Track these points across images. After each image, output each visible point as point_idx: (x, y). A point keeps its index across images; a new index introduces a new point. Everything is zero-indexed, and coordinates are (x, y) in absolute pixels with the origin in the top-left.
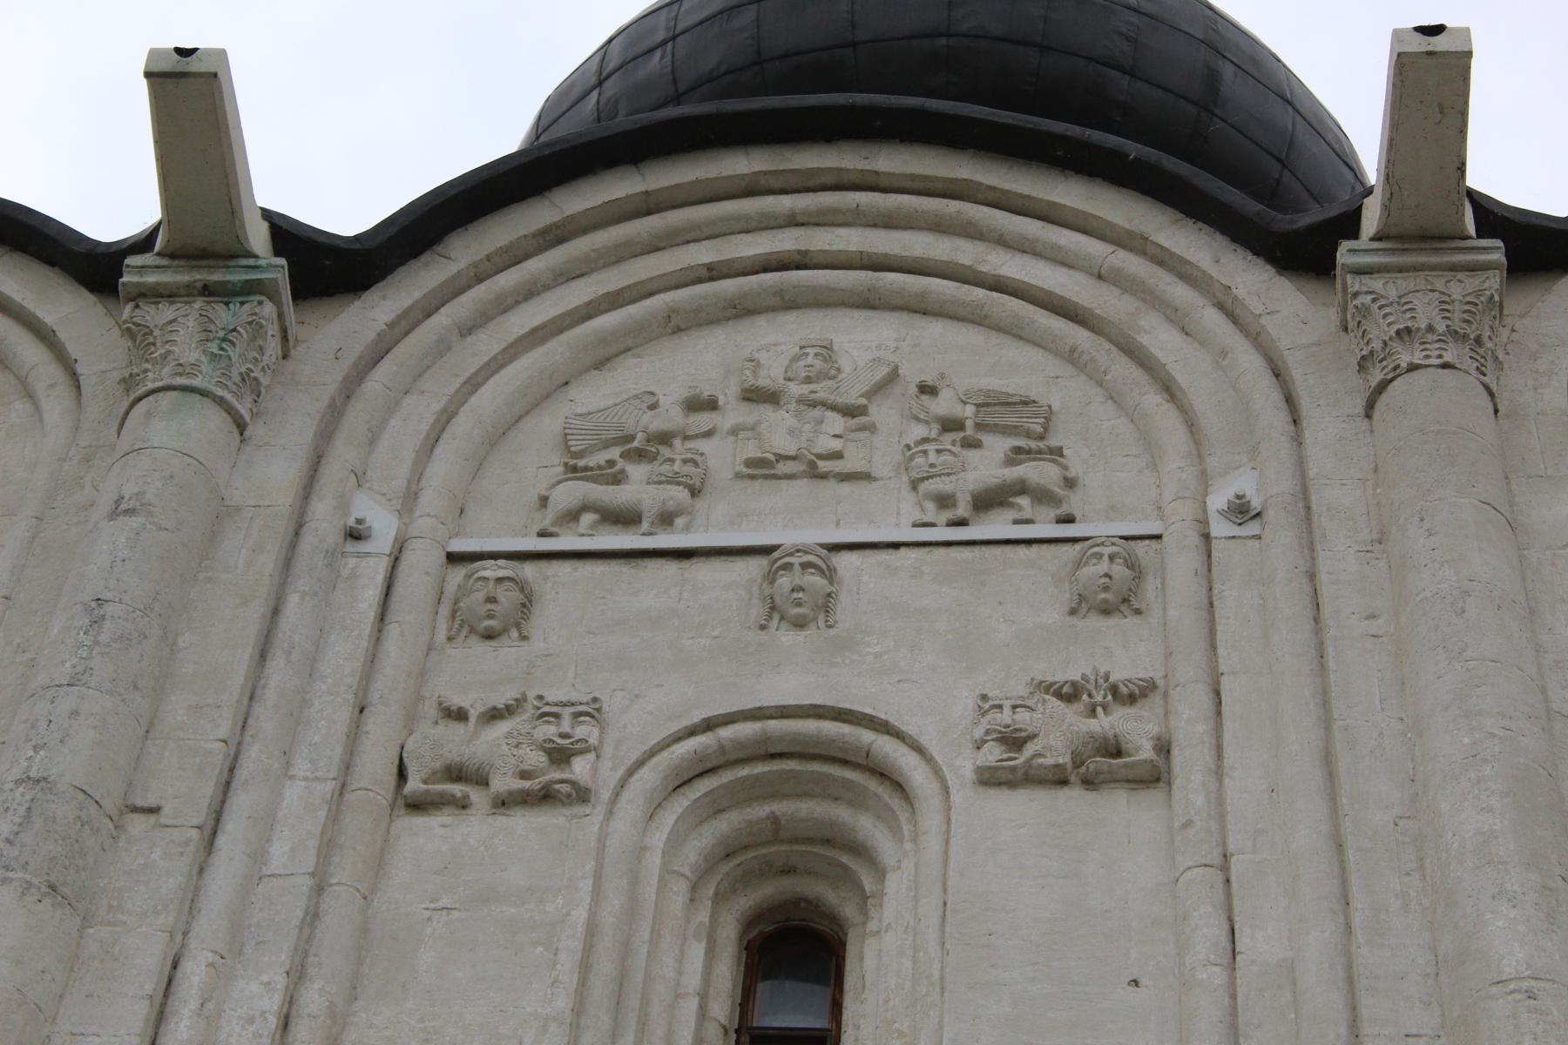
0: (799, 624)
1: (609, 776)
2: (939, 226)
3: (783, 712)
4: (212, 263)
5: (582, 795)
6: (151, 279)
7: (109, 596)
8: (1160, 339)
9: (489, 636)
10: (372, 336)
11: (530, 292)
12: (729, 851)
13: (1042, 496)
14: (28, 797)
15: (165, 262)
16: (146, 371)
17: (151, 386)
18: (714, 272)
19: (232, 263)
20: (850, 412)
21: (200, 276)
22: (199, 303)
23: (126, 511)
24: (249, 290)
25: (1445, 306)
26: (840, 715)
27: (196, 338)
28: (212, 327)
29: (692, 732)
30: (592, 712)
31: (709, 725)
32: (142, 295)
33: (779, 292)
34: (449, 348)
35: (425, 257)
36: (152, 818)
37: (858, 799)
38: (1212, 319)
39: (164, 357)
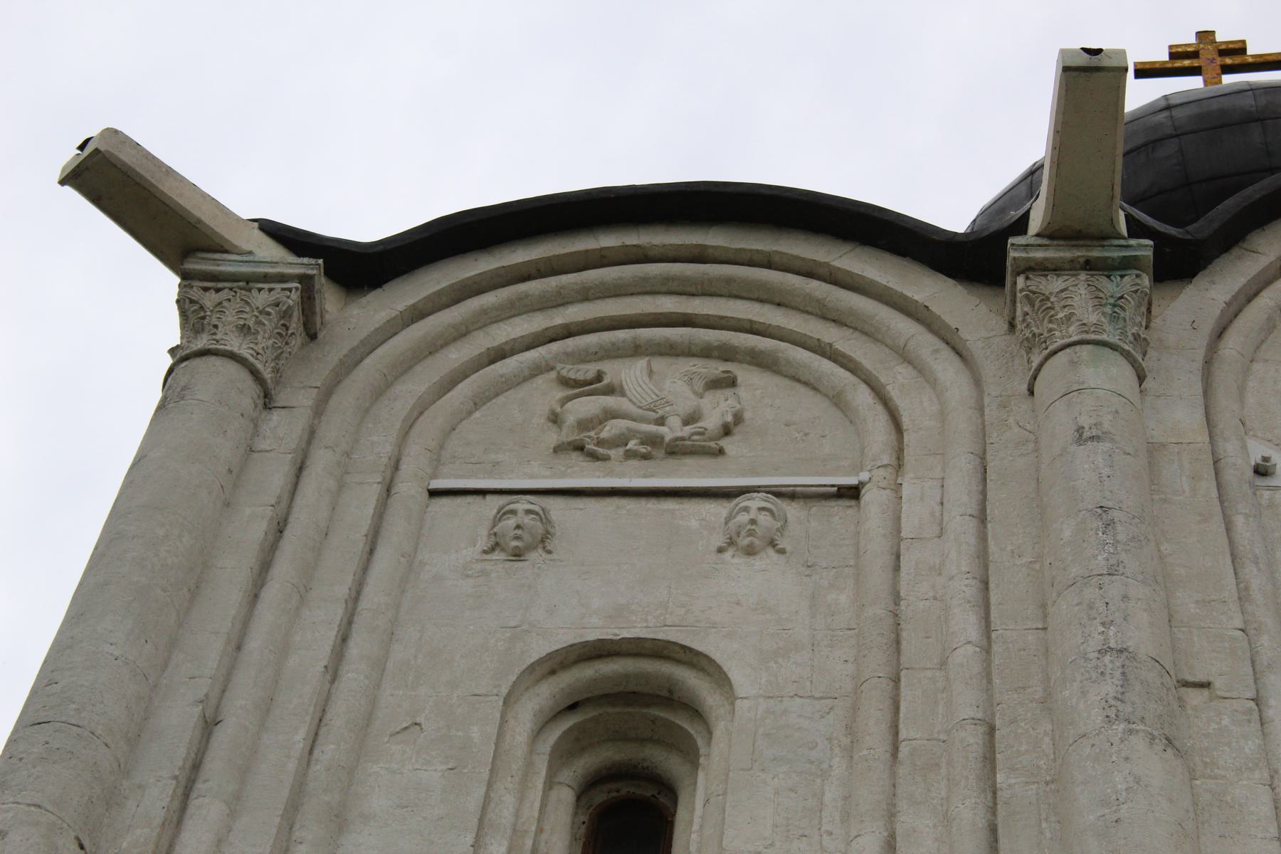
4: (1089, 243)
6: (1039, 254)
7: (1110, 504)
10: (1218, 312)
14: (1118, 664)
15: (1040, 241)
16: (1050, 330)
17: (1060, 342)
19: (1106, 243)
21: (1080, 253)
22: (1083, 276)
23: (1092, 438)
24: (1126, 265)
27: (1090, 304)
28: (1101, 295)
32: (1031, 269)
34: (1274, 327)
35: (1236, 251)
36: (1205, 692)
39: (1069, 317)
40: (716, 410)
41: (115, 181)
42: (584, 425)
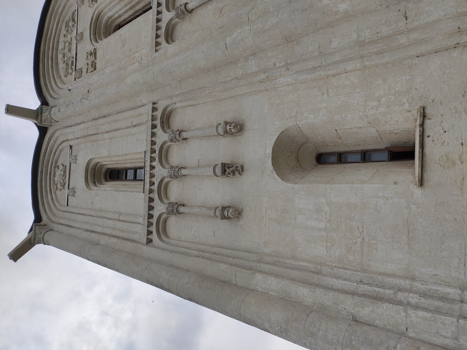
3: (90, 32)
29: (91, 42)
31: (91, 40)
37: (101, 23)
40: (61, 167)
41: (16, 255)
42: (61, 186)
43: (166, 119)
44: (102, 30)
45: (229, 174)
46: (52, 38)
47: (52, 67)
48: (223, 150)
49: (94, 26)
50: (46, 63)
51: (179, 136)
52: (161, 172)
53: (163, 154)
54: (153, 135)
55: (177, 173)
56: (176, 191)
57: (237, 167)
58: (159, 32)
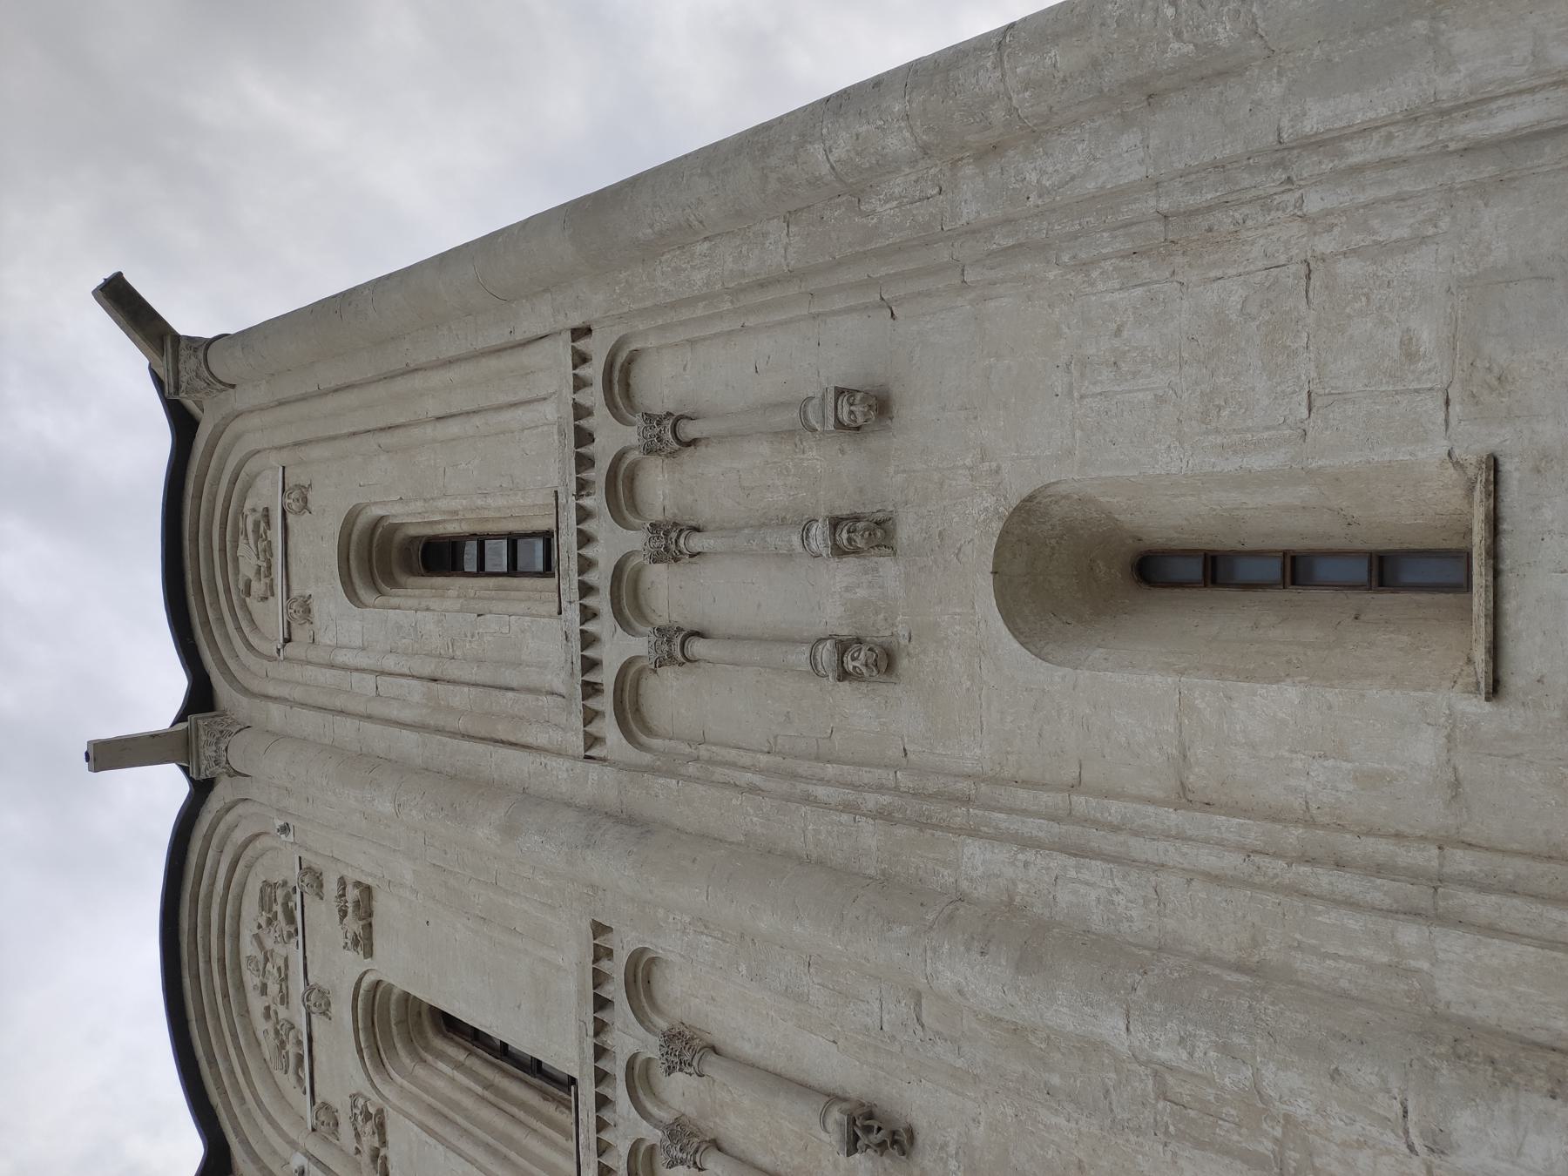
0: (329, 1004)
1: (375, 1097)
2: (208, 907)
3: (355, 1020)
5: (380, 1111)
8: (239, 836)
9: (337, 1124)
11: (232, 1072)
12: (409, 1042)
13: (288, 898)
18: (226, 995)
20: (267, 960)
25: (208, 744)
26: (355, 999)
29: (362, 1058)
30: (354, 1097)
31: (360, 1051)
33: (233, 971)
38: (230, 818)
43: (620, 379)
44: (392, 1012)
45: (868, 1146)
46: (216, 900)
47: (226, 995)
48: (832, 594)
49: (365, 1004)
50: (207, 982)
51: (673, 434)
52: (613, 542)
53: (622, 488)
54: (588, 640)
55: (672, 540)
56: (670, 592)
57: (894, 1133)
58: (588, 475)
